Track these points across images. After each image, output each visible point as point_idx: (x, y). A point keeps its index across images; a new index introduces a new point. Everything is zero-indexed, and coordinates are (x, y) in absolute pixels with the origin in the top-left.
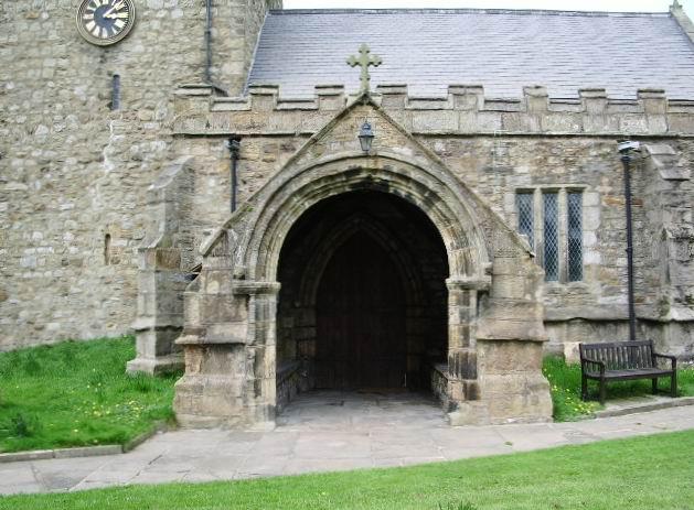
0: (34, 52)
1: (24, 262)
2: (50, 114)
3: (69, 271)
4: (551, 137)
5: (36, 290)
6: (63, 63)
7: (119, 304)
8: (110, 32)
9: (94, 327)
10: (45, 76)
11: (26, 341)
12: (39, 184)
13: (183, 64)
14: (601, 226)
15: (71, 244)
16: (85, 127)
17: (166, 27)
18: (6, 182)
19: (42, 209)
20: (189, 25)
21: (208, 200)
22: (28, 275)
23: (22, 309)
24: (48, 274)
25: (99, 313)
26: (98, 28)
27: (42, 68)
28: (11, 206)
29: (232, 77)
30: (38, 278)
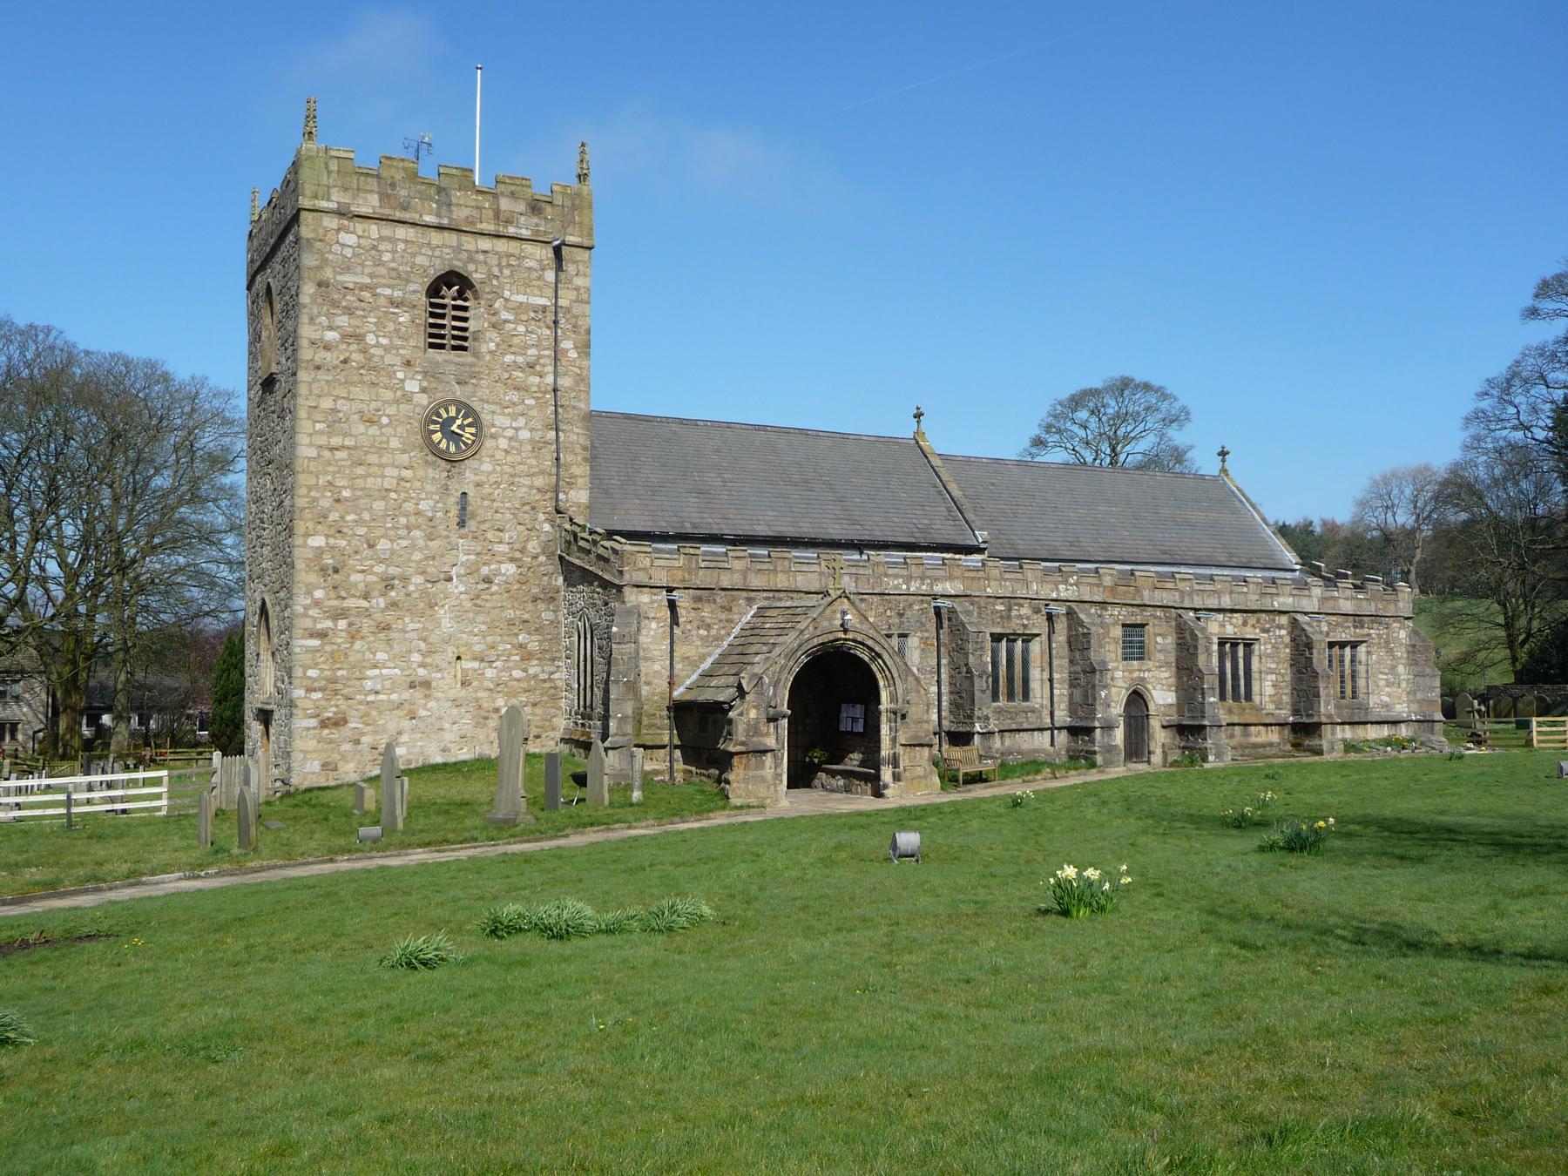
0: (373, 458)
1: (369, 684)
2: (394, 528)
3: (418, 694)
4: (889, 594)
5: (380, 712)
6: (407, 474)
7: (470, 726)
8: (458, 447)
9: (444, 750)
10: (386, 486)
11: (368, 768)
12: (382, 602)
13: (531, 487)
15: (420, 666)
16: (431, 544)
18: (344, 598)
19: (388, 628)
20: (537, 445)
21: (649, 640)
22: (371, 698)
23: (364, 734)
24: (394, 697)
25: (448, 736)
26: (444, 440)
27: (383, 477)
28: (351, 624)
29: (579, 505)
30: (382, 701)
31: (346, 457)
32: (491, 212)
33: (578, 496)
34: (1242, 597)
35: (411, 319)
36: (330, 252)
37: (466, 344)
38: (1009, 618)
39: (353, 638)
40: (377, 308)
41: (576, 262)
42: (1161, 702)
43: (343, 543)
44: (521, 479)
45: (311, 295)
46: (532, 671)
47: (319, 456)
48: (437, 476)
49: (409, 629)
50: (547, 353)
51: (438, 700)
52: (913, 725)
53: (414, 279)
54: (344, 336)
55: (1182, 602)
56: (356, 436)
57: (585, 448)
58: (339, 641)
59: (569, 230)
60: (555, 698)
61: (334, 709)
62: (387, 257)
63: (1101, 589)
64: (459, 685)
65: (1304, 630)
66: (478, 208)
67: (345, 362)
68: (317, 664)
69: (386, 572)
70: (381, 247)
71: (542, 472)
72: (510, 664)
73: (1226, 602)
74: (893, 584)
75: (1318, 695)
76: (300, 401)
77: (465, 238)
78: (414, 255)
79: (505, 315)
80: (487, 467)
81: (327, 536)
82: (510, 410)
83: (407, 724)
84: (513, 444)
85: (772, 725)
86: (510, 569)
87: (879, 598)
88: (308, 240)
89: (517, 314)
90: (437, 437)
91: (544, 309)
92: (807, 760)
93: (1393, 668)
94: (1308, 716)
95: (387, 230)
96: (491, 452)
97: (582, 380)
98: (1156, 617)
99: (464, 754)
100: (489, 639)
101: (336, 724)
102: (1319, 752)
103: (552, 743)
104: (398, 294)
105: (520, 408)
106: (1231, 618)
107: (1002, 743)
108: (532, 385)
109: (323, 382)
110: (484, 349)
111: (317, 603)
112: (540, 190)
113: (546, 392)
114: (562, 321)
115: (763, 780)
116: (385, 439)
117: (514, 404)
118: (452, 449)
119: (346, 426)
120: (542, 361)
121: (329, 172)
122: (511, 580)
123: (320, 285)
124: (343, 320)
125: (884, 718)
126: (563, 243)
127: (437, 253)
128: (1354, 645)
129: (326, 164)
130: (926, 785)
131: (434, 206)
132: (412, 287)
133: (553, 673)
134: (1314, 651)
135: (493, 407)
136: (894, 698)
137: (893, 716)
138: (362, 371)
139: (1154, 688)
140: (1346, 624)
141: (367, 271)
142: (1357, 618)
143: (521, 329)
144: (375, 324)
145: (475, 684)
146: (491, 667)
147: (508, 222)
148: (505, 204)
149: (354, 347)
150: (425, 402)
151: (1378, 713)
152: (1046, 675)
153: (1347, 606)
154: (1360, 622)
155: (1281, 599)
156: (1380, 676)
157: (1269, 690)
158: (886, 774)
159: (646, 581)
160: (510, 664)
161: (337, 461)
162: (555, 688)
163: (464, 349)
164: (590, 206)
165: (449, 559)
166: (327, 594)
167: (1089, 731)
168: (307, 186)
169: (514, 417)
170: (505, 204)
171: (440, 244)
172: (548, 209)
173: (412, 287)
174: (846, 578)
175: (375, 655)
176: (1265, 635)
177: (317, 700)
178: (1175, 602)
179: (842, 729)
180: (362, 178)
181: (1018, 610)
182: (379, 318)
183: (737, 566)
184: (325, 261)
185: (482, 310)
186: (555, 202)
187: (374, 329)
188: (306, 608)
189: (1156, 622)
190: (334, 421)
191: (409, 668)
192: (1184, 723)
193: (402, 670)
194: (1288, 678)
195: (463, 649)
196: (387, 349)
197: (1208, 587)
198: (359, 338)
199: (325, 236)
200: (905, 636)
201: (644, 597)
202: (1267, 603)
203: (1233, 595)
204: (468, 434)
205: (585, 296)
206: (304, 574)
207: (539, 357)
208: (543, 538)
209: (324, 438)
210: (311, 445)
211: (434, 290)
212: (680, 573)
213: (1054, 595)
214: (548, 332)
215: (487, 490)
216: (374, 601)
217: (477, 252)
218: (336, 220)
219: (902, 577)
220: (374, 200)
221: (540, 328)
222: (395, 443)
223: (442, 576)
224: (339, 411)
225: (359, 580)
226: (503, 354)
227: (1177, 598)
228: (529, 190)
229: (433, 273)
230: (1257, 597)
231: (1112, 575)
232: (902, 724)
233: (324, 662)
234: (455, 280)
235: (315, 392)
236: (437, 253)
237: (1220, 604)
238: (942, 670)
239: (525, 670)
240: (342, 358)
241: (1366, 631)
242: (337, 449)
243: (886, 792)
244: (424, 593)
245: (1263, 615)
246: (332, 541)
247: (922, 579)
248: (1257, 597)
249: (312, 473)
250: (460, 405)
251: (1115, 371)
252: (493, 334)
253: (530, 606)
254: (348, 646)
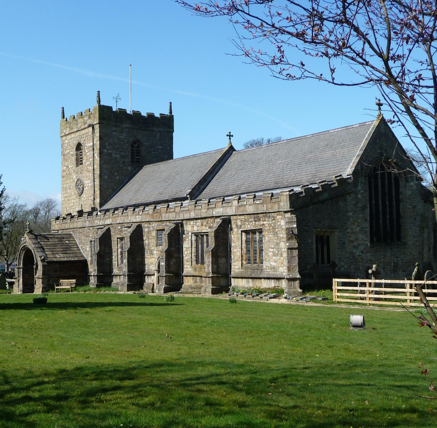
34: (199, 211)
55: (176, 217)
73: (193, 215)
93: (278, 244)
140: (250, 220)
142: (256, 215)
151: (267, 271)
153: (250, 209)
154: (258, 217)
156: (270, 250)
203: (196, 211)
230: (205, 211)
237: (190, 216)
241: (262, 223)
245: (210, 219)
248: (205, 211)
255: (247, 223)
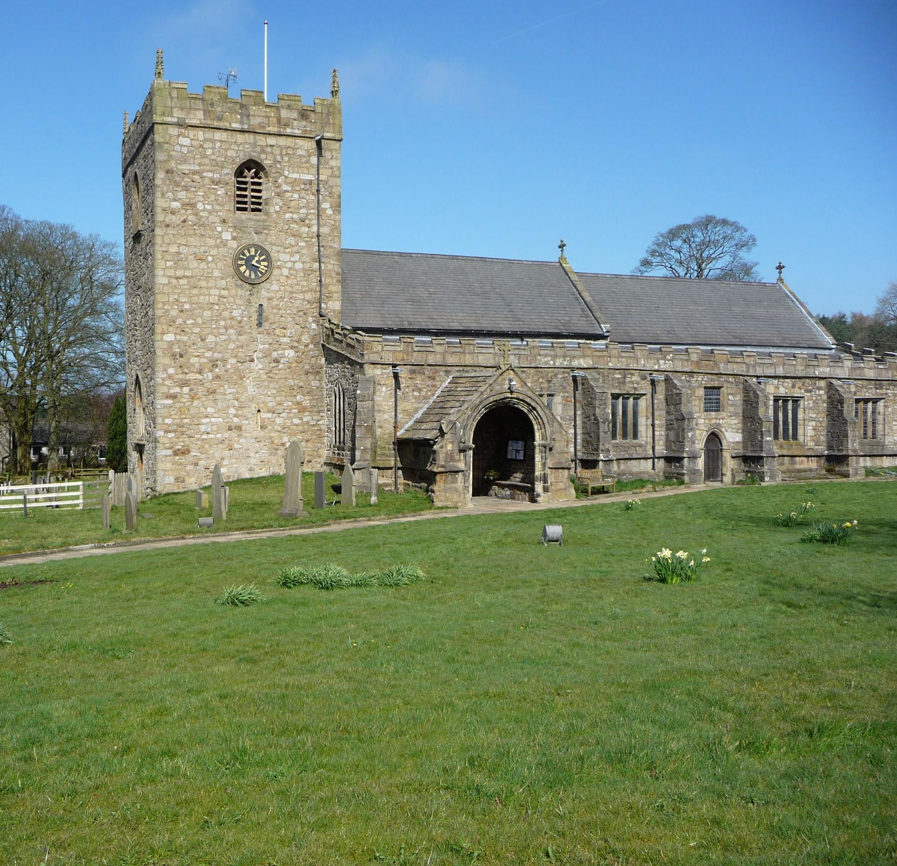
3: (234, 434)
4: (541, 368)
5: (210, 446)
8: (256, 275)
9: (250, 470)
11: (203, 481)
12: (210, 376)
13: (304, 300)
14: (563, 413)
15: (234, 416)
16: (240, 338)
17: (292, 275)
18: (187, 373)
19: (214, 392)
20: (307, 273)
22: (204, 437)
24: (219, 436)
25: (253, 461)
26: (248, 271)
27: (209, 295)
28: (191, 390)
29: (334, 311)
31: (186, 283)
32: (275, 120)
33: (334, 305)
34: (792, 368)
35: (225, 193)
36: (174, 150)
37: (260, 207)
38: (624, 383)
39: (193, 398)
40: (204, 186)
41: (331, 150)
42: (731, 440)
43: (186, 338)
44: (297, 295)
45: (162, 179)
46: (305, 419)
47: (169, 283)
48: (243, 294)
49: (227, 393)
50: (313, 211)
51: (246, 438)
52: (557, 455)
53: (226, 166)
54: (183, 205)
55: (748, 371)
56: (192, 270)
57: (338, 274)
58: (184, 400)
59: (326, 129)
60: (320, 437)
61: (182, 444)
62: (209, 152)
63: (690, 363)
64: (259, 429)
65: (837, 390)
66: (266, 117)
67: (184, 221)
68: (171, 415)
69: (212, 356)
70: (206, 146)
71: (311, 290)
72: (292, 415)
73: (780, 371)
74: (545, 360)
75: (846, 436)
76: (157, 248)
77: (258, 137)
78: (226, 150)
79: (285, 187)
80: (275, 287)
81: (176, 334)
82: (289, 250)
83: (227, 453)
84: (291, 272)
85: (462, 454)
86: (290, 353)
87: (534, 370)
88: (159, 143)
89: (293, 186)
90: (243, 268)
91: (311, 182)
92: (486, 477)
94: (839, 450)
95: (209, 134)
96: (277, 278)
97: (336, 228)
98: (728, 382)
99: (263, 473)
100: (278, 399)
101: (183, 453)
102: (847, 476)
103: (319, 465)
104: (216, 176)
105: (296, 248)
106: (783, 382)
107: (619, 468)
108: (303, 233)
109: (171, 236)
110: (272, 210)
111: (170, 377)
112: (306, 102)
113: (312, 238)
114: (323, 190)
115: (456, 490)
116: (210, 271)
117: (292, 245)
118: (253, 276)
119: (186, 263)
120: (309, 217)
121: (172, 98)
122: (291, 360)
123: (167, 172)
124: (182, 195)
125: (537, 450)
126: (323, 138)
127: (241, 148)
128: (875, 401)
129: (170, 93)
130: (566, 495)
131: (239, 117)
132: (225, 171)
133: (318, 421)
134: (845, 405)
135: (278, 248)
136: (544, 437)
137: (544, 449)
138: (195, 227)
139: (726, 431)
140: (869, 386)
141: (196, 162)
142: (878, 382)
143: (296, 196)
144: (203, 196)
145: (269, 427)
146: (279, 417)
147: (287, 125)
148: (284, 113)
149: (189, 212)
150: (235, 246)
152: (650, 422)
153: (870, 374)
154: (880, 385)
155: (821, 369)
157: (810, 432)
158: (539, 487)
159: (378, 360)
160: (292, 415)
161: (180, 286)
162: (320, 430)
163: (259, 210)
164: (340, 112)
165: (252, 347)
166: (176, 371)
167: (680, 460)
168: (158, 108)
169: (292, 254)
170: (284, 113)
171: (243, 142)
172: (312, 115)
173: (225, 171)
174: (512, 357)
175: (206, 409)
176: (809, 394)
177: (172, 438)
178: (743, 371)
179: (509, 457)
180: (193, 101)
181: (631, 378)
182: (204, 192)
183: (439, 350)
184: (170, 157)
185: (270, 184)
186: (317, 111)
187: (202, 199)
188: (163, 380)
189: (729, 385)
190: (178, 259)
191: (228, 418)
192: (747, 454)
193: (224, 419)
194: (824, 424)
195: (261, 406)
196: (210, 213)
197: (767, 361)
198: (193, 205)
199: (170, 140)
200: (552, 395)
201: (378, 371)
202: (811, 372)
204: (263, 266)
205: (337, 173)
206: (162, 358)
207: (307, 214)
208: (312, 333)
209: (173, 271)
210: (164, 275)
211: (239, 173)
212: (401, 355)
213: (656, 367)
214: (313, 198)
215: (275, 302)
216: (205, 375)
217: (267, 146)
218: (176, 130)
219: (550, 356)
220: (200, 114)
221: (308, 195)
222: (216, 273)
223: (248, 358)
224: (181, 254)
225: (195, 361)
226: (284, 213)
227: (744, 369)
228: (299, 103)
229: (239, 161)
230: (803, 368)
231: (697, 353)
232: (550, 454)
233: (175, 414)
234: (253, 165)
235: (166, 241)
236: (241, 148)
237: (775, 372)
238: (578, 418)
239: (301, 419)
240: (182, 219)
241: (884, 391)
242: (180, 278)
243: (538, 499)
244: (237, 369)
245: (807, 380)
246: (178, 337)
247: (564, 357)
248: (803, 368)
249: (164, 293)
250: (258, 247)
251: (702, 211)
252: (278, 200)
253: (304, 377)
254: (190, 403)
255: (865, 390)
